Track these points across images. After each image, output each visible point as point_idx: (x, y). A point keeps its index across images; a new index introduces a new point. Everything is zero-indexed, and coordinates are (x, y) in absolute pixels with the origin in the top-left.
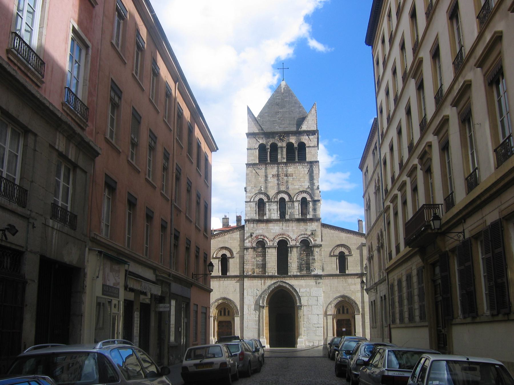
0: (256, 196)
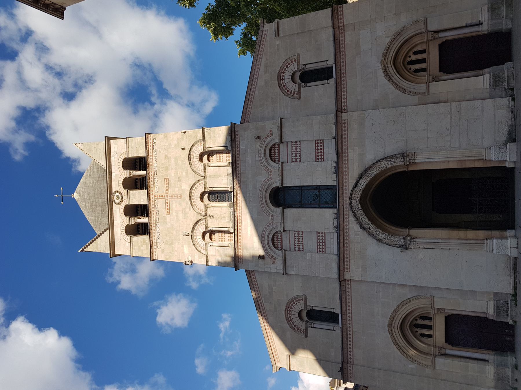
0: (198, 244)
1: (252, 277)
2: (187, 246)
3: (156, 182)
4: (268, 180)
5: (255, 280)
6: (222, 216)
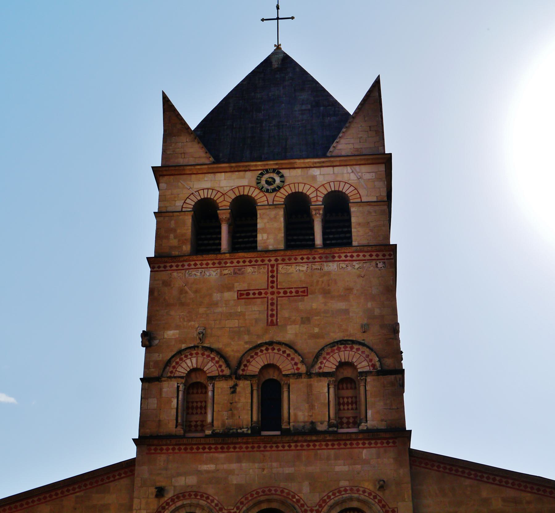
1: (122, 472)
2: (177, 336)
3: (301, 269)
4: (302, 505)
5: (117, 477)
6: (235, 412)
